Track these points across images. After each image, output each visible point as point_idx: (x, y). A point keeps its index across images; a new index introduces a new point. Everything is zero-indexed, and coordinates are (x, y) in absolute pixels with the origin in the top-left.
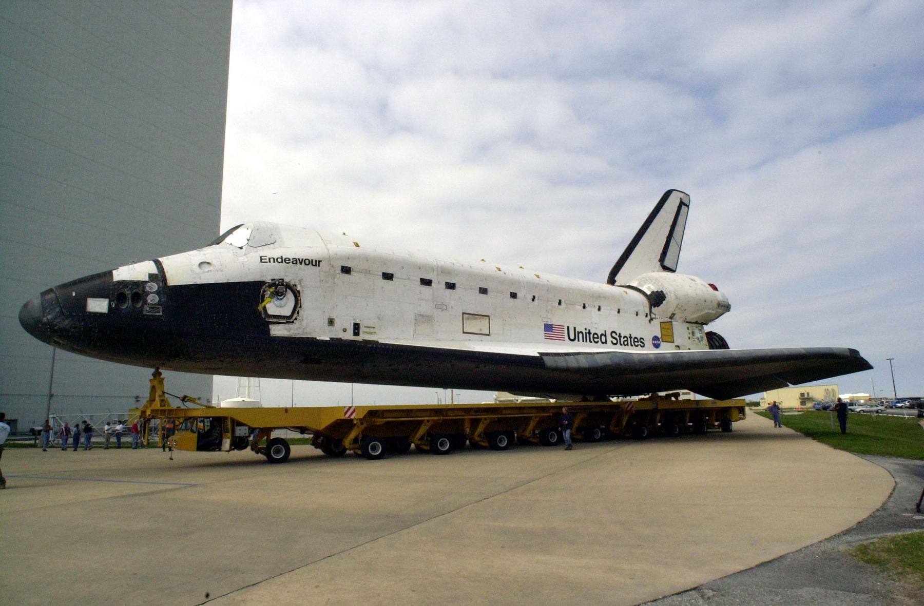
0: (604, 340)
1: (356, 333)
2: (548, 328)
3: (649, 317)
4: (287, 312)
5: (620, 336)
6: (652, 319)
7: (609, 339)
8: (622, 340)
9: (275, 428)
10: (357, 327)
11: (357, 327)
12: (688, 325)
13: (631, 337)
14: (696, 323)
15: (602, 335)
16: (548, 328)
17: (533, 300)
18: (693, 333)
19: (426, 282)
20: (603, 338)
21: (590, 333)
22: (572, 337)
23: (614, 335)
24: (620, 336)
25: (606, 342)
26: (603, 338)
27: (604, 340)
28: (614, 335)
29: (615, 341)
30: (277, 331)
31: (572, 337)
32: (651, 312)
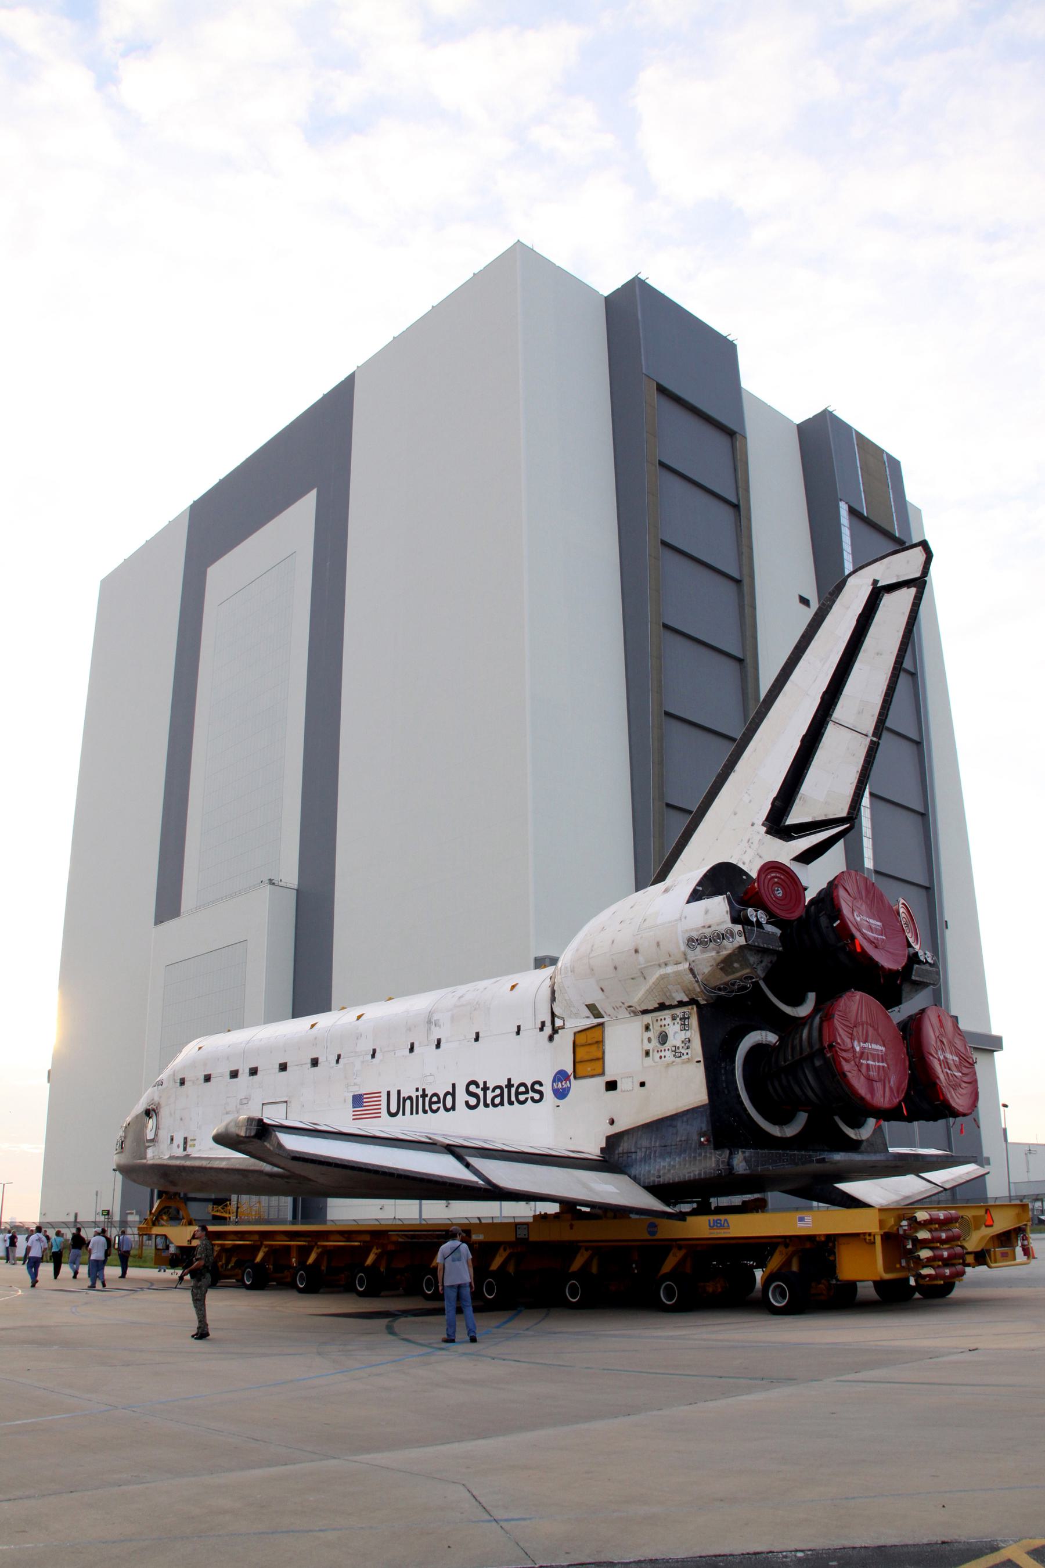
0: (449, 1105)
1: (185, 1149)
3: (548, 1030)
5: (485, 1089)
6: (555, 1031)
7: (461, 1096)
8: (490, 1095)
9: (561, 1270)
12: (647, 1019)
13: (509, 1085)
14: (662, 1007)
15: (447, 1093)
16: (358, 1100)
18: (663, 1038)
19: (234, 1074)
20: (449, 1098)
21: (424, 1096)
22: (393, 1109)
23: (473, 1088)
24: (485, 1089)
25: (453, 1108)
26: (449, 1098)
27: (449, 1105)
28: (473, 1088)
29: (473, 1101)
31: (393, 1109)
32: (553, 1015)
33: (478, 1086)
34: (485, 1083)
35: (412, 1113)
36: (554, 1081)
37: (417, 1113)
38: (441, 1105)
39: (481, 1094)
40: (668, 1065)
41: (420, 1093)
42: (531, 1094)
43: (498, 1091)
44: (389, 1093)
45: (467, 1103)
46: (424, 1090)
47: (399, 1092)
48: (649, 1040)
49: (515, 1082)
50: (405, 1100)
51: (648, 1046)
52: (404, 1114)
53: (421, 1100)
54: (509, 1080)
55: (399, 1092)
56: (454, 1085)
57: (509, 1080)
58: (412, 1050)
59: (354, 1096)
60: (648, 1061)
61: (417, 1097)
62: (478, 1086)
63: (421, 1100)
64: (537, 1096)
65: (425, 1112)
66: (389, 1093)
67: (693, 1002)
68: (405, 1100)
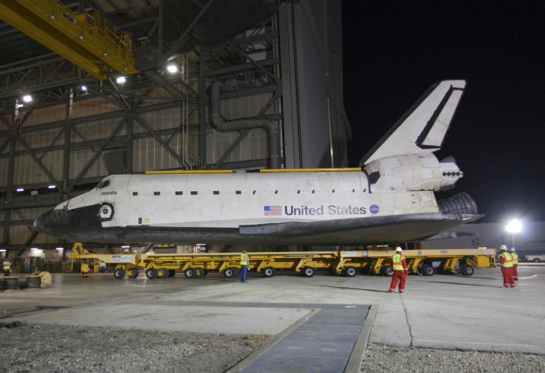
1: (139, 223)
2: (267, 208)
4: (108, 216)
7: (326, 209)
8: (340, 211)
10: (140, 220)
11: (140, 220)
14: (422, 190)
15: (318, 209)
16: (267, 208)
17: (254, 193)
22: (289, 211)
25: (322, 213)
30: (105, 224)
31: (289, 211)
33: (334, 207)
34: (338, 207)
35: (300, 214)
36: (371, 208)
37: (303, 214)
38: (316, 212)
39: (336, 210)
40: (423, 207)
41: (304, 207)
42: (360, 211)
43: (344, 209)
44: (286, 207)
45: (329, 212)
46: (306, 207)
47: (292, 207)
48: (414, 199)
49: (353, 207)
50: (295, 210)
51: (414, 201)
52: (295, 214)
53: (304, 211)
54: (350, 206)
55: (292, 207)
56: (322, 206)
57: (350, 206)
58: (299, 192)
59: (265, 207)
60: (414, 205)
61: (302, 209)
62: (334, 207)
63: (304, 211)
64: (363, 212)
65: (306, 214)
66: (286, 207)
67: (434, 190)
68: (295, 210)
